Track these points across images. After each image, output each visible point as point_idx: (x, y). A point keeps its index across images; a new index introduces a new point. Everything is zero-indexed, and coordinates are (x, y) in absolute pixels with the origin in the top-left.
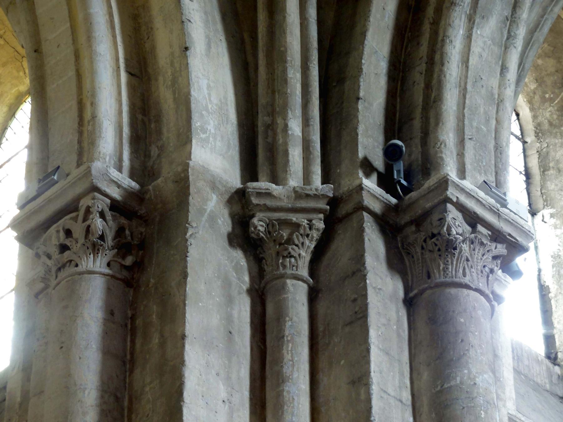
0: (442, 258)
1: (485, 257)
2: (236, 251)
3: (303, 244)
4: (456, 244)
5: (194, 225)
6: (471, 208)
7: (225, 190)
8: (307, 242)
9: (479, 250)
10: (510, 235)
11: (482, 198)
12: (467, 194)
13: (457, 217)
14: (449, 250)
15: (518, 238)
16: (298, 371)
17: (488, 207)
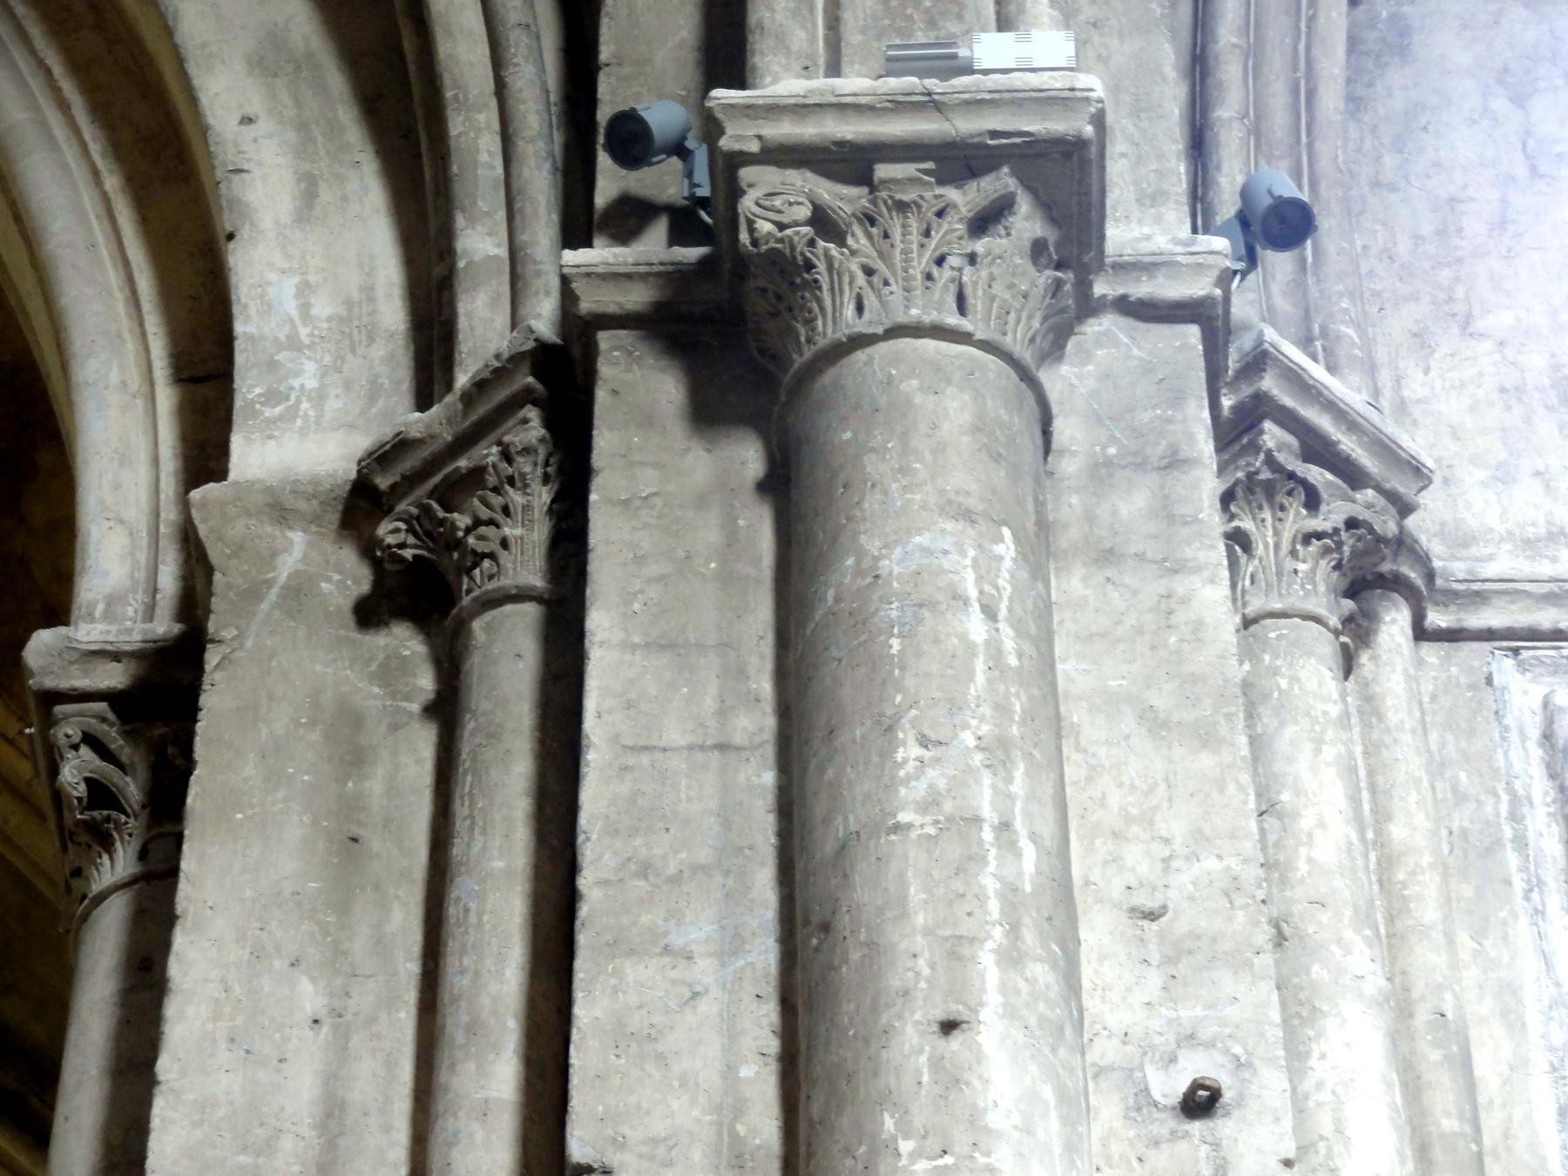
0: (796, 312)
1: (936, 236)
2: (384, 631)
3: (506, 511)
4: (802, 254)
5: (227, 634)
6: (817, 140)
7: (321, 503)
8: (516, 497)
9: (904, 226)
10: (994, 134)
11: (855, 95)
12: (795, 113)
13: (783, 184)
14: (798, 281)
15: (1025, 129)
16: (484, 832)
17: (889, 105)
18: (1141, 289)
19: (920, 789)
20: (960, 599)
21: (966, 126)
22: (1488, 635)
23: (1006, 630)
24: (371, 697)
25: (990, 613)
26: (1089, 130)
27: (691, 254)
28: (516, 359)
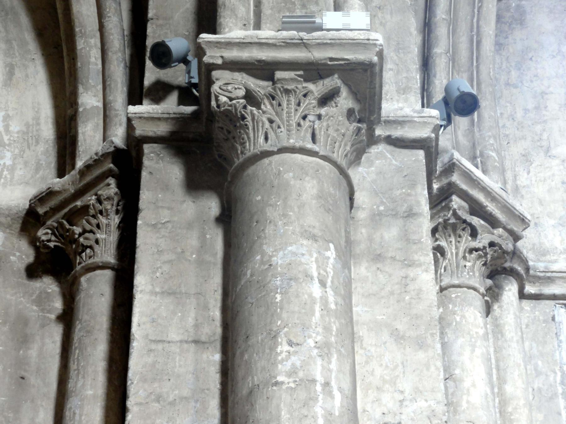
0: (237, 139)
1: (303, 106)
2: (39, 280)
3: (98, 226)
4: (240, 112)
6: (249, 59)
7: (12, 219)
8: (103, 220)
9: (288, 101)
10: (331, 59)
11: (267, 39)
12: (239, 46)
13: (233, 79)
14: (238, 124)
15: (346, 57)
16: (84, 377)
17: (283, 44)
18: (397, 133)
19: (288, 366)
20: (308, 277)
21: (318, 55)
22: (554, 297)
23: (330, 292)
24: (32, 311)
25: (323, 284)
26: (375, 59)
27: (189, 109)
28: (105, 156)
